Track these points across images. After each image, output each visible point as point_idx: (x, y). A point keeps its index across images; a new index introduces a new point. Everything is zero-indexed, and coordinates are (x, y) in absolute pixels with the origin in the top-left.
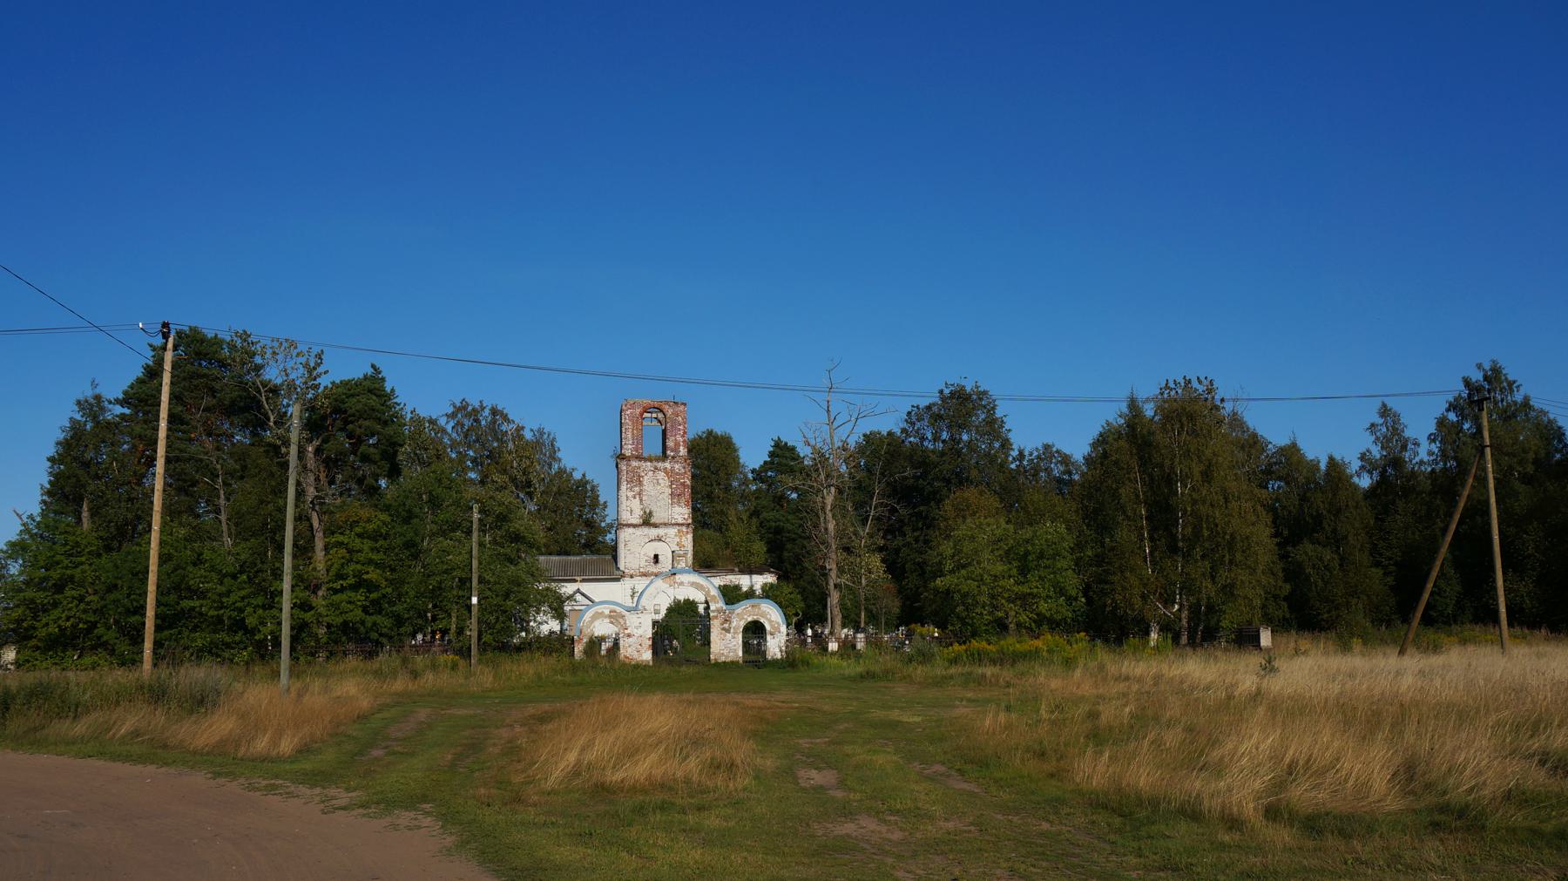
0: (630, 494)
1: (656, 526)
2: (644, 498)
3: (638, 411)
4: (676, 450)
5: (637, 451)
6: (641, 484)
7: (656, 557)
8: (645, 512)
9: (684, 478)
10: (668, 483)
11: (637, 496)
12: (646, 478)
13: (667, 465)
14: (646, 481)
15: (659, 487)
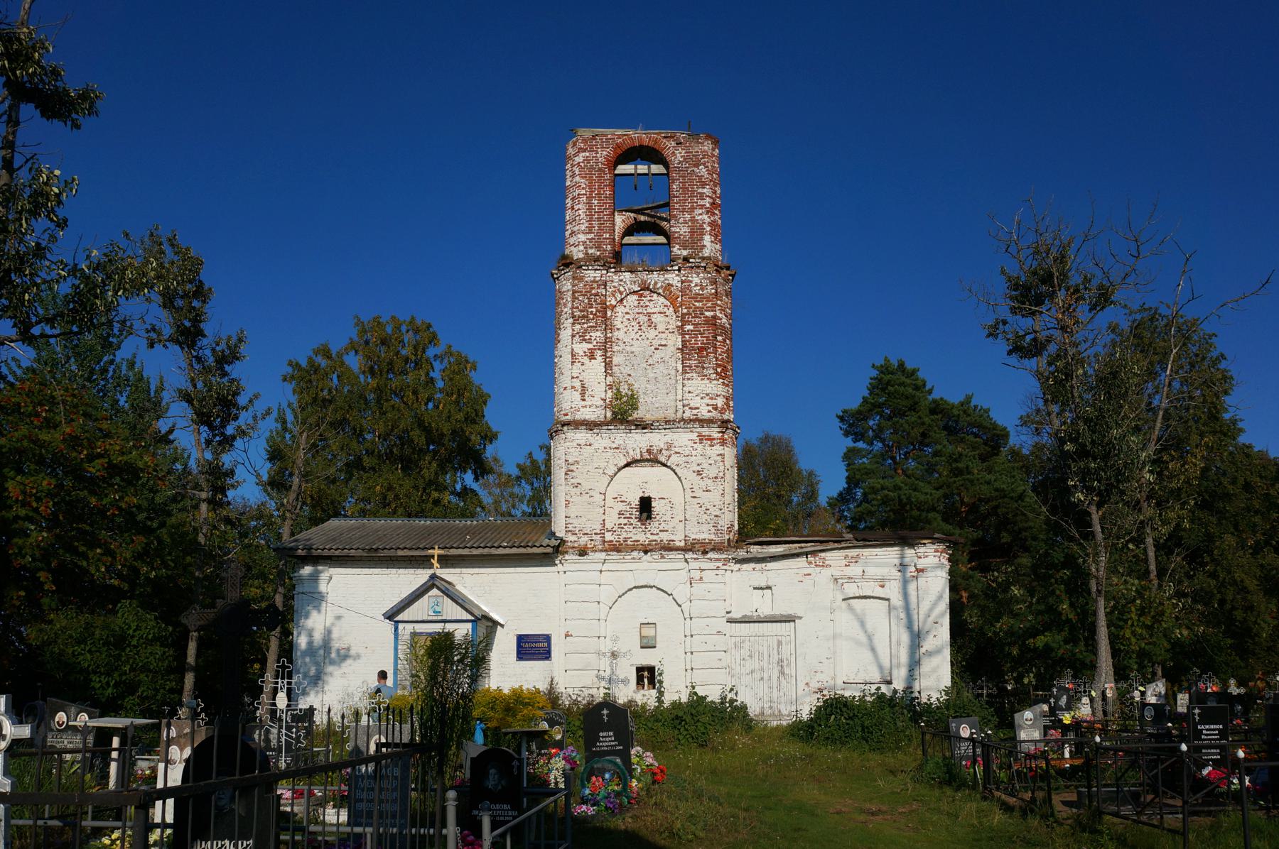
0: (581, 348)
1: (643, 426)
2: (616, 360)
3: (603, 155)
4: (694, 241)
5: (598, 248)
6: (607, 325)
7: (645, 506)
8: (618, 395)
9: (713, 309)
10: (674, 323)
12: (620, 309)
13: (674, 279)
14: (619, 318)
15: (652, 333)
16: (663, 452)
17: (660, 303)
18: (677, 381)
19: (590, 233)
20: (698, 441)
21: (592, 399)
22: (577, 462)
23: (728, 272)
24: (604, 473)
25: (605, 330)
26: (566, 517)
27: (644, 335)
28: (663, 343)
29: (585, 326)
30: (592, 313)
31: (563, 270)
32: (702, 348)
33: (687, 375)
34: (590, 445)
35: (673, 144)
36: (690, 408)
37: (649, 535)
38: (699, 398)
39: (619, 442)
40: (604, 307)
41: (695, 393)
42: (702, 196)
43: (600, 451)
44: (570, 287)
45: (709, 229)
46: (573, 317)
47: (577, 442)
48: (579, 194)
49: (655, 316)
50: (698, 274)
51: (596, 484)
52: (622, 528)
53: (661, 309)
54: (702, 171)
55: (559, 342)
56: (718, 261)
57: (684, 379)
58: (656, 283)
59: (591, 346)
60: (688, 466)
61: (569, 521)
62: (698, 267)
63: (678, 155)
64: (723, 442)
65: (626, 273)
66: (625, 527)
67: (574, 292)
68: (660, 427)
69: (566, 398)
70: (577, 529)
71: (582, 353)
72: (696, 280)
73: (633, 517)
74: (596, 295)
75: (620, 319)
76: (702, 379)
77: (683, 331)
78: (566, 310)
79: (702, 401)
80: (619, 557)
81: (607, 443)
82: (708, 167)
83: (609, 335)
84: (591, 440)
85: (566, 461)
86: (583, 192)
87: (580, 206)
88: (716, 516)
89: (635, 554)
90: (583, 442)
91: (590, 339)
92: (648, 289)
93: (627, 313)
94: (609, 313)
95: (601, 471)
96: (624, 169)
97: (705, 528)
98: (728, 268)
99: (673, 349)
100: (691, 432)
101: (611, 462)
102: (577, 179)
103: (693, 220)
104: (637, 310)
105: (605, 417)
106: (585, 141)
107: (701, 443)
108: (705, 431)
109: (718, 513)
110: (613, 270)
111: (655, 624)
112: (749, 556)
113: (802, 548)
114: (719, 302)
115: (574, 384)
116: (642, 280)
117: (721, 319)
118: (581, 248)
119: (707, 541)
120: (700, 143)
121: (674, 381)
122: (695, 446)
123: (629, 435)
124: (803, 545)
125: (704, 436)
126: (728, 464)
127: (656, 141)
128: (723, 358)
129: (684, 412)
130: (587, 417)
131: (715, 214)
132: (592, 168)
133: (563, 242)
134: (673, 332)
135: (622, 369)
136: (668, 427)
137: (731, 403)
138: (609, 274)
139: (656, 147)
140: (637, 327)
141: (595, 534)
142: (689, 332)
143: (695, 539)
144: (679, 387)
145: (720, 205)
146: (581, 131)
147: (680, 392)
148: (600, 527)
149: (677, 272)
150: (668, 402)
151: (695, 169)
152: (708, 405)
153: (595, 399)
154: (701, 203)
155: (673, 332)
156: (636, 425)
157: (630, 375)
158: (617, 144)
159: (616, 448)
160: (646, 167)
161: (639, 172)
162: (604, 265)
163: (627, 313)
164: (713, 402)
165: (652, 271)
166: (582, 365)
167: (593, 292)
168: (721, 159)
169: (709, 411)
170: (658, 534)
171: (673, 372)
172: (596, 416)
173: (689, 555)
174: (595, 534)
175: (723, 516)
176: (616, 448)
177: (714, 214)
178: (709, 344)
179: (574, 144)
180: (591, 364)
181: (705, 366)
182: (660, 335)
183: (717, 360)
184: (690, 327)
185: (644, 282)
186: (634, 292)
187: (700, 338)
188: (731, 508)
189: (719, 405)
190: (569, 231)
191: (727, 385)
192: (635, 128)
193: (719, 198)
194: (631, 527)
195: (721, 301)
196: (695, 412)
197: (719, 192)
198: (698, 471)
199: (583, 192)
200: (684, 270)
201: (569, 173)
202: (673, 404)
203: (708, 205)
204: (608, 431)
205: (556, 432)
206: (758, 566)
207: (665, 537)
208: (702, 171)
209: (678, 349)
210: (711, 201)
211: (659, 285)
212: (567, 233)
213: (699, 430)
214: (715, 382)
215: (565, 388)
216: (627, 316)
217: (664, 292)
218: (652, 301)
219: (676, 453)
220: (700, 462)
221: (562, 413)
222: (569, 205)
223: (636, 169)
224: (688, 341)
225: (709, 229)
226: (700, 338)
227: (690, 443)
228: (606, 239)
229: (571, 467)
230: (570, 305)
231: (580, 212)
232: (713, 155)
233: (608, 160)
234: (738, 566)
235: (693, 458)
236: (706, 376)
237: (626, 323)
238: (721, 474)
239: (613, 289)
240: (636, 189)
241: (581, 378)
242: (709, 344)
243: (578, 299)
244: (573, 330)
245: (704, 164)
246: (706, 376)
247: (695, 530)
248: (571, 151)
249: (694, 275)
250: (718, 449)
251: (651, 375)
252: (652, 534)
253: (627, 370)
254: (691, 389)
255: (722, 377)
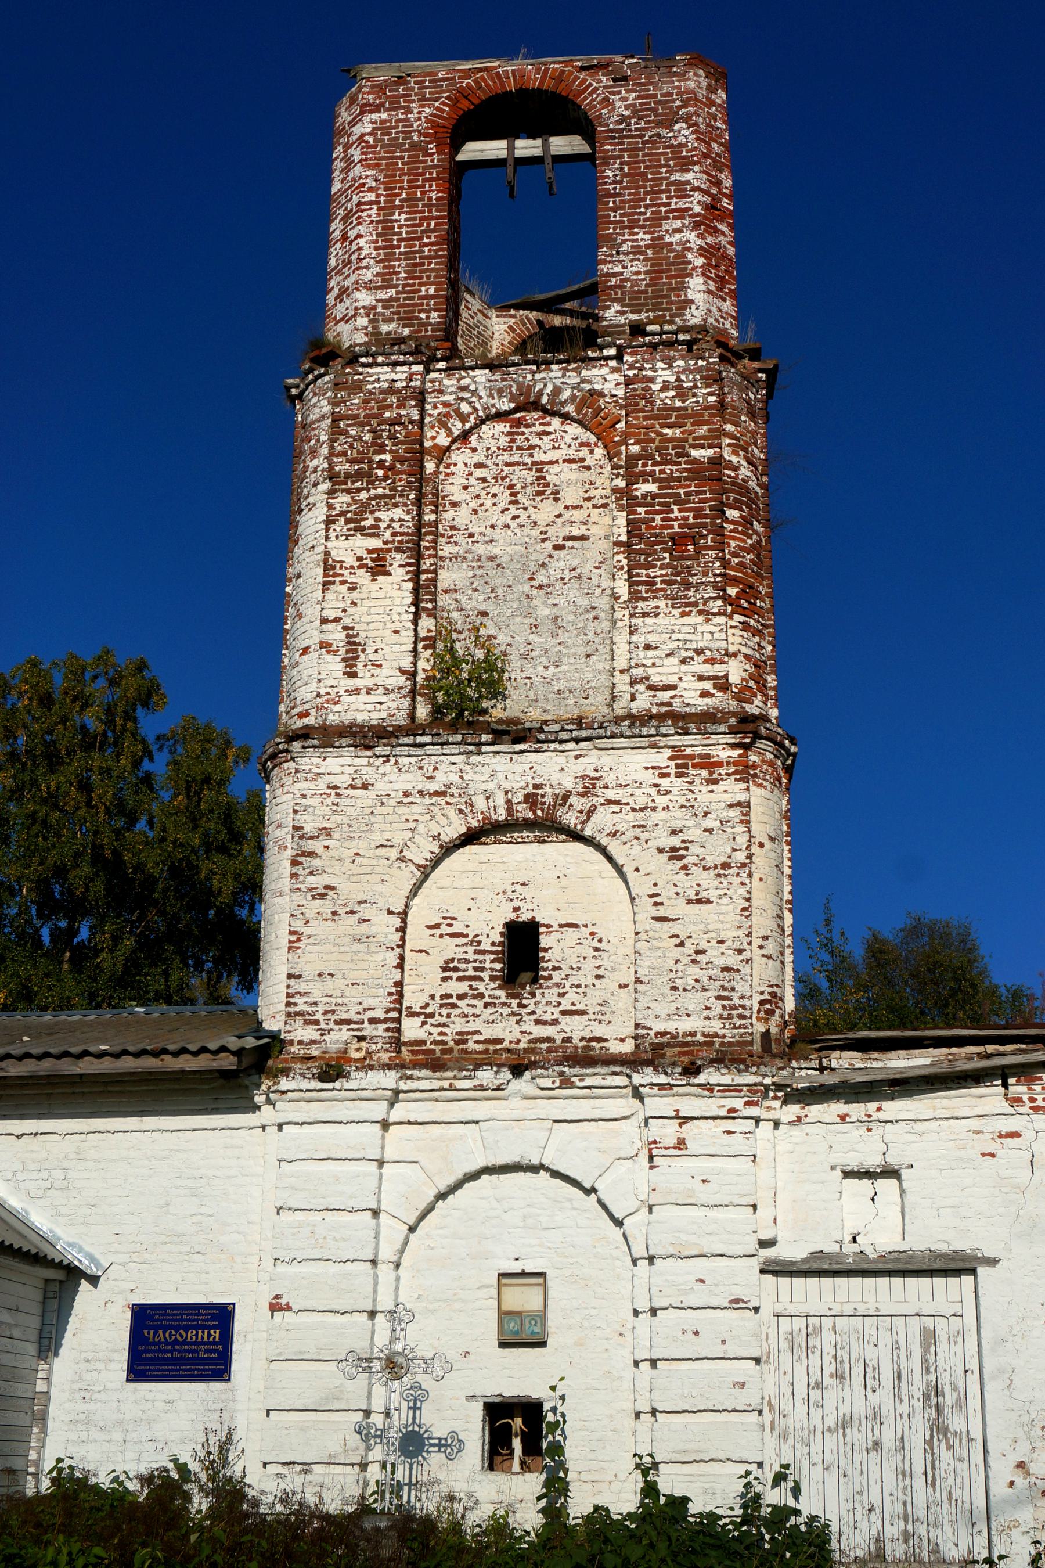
2: (445, 578)
5: (407, 319)
9: (713, 440)
11: (397, 560)
12: (460, 457)
15: (547, 510)
16: (573, 800)
17: (568, 439)
18: (614, 622)
19: (387, 285)
20: (672, 771)
21: (376, 671)
22: (327, 832)
23: (756, 365)
24: (402, 859)
25: (419, 502)
26: (290, 976)
27: (524, 515)
28: (576, 532)
29: (364, 495)
30: (381, 464)
31: (311, 370)
32: (683, 536)
33: (641, 604)
34: (365, 787)
35: (605, 81)
36: (650, 688)
37: (529, 1026)
38: (674, 661)
39: (442, 779)
40: (417, 453)
41: (666, 649)
42: (682, 190)
43: (392, 802)
44: (327, 409)
45: (700, 261)
46: (333, 476)
47: (331, 778)
48: (359, 204)
49: (555, 469)
50: (669, 362)
51: (380, 888)
52: (454, 1006)
53: (572, 453)
54: (683, 133)
55: (296, 542)
56: (728, 335)
57: (632, 616)
58: (557, 391)
59: (376, 543)
60: (644, 836)
61: (298, 986)
62: (671, 344)
63: (618, 104)
64: (745, 772)
65: (478, 372)
66: (460, 1003)
67: (336, 418)
68: (564, 735)
69: (305, 673)
70: (321, 1009)
71: (350, 561)
72: (665, 375)
73: (485, 975)
74: (393, 423)
75: (459, 480)
76: (683, 615)
77: (631, 497)
78: (315, 462)
79: (684, 668)
80: (436, 1084)
81: (412, 780)
82: (696, 124)
83: (429, 517)
84: (369, 774)
85: (296, 828)
86: (371, 197)
87: (362, 229)
88: (727, 969)
89: (486, 1076)
90: (343, 780)
91: (377, 527)
92: (535, 405)
93: (479, 465)
94: (430, 466)
95: (394, 854)
96: (475, 150)
97: (693, 1001)
98: (755, 355)
99: (604, 545)
100: (653, 746)
101: (421, 828)
102: (358, 170)
103: (658, 245)
104: (506, 457)
105: (412, 715)
106: (379, 89)
107: (679, 775)
108: (694, 744)
109: (733, 960)
110: (442, 365)
111: (542, 1275)
112: (829, 1079)
113: (989, 1056)
114: (729, 427)
115: (328, 637)
116: (519, 384)
117: (736, 469)
118: (363, 321)
119: (699, 1038)
120: (676, 74)
121: (606, 625)
122: (665, 782)
123: (474, 759)
124: (991, 1049)
125: (692, 757)
126: (760, 831)
127: (560, 78)
128: (741, 564)
129: (633, 698)
130: (360, 718)
131: (716, 231)
132: (395, 144)
133: (319, 312)
134: (605, 506)
135: (464, 600)
136: (584, 734)
137: (771, 680)
138: (433, 375)
139: (561, 89)
140: (505, 497)
141: (373, 1021)
142: (647, 499)
143: (658, 1034)
144: (621, 638)
145: (731, 214)
146: (368, 70)
147: (622, 649)
148: (386, 1002)
149: (613, 363)
150: (589, 676)
151: (664, 132)
152: (701, 678)
153: (385, 671)
154: (682, 204)
155: (605, 506)
156: (494, 732)
157: (484, 614)
158: (460, 90)
159: (437, 794)
160: (538, 142)
161: (519, 153)
162: (417, 352)
163: (479, 465)
164: (718, 670)
165: (548, 363)
166: (353, 588)
167: (387, 415)
168: (733, 113)
169: (705, 694)
170: (555, 1022)
171: (604, 603)
172: (384, 715)
173: (646, 1077)
174: (373, 1021)
175: (746, 969)
176: (437, 794)
177: (716, 231)
178: (704, 526)
179: (353, 100)
180: (375, 586)
181: (693, 580)
182: (567, 515)
183: (725, 564)
184: (652, 487)
185: (525, 390)
186: (500, 416)
187: (676, 513)
188: (771, 947)
189: (734, 678)
190: (336, 291)
191: (756, 633)
192: (508, 54)
193: (725, 195)
194: (480, 1003)
195: (736, 424)
196: (664, 696)
197: (728, 183)
198: (674, 849)
199: (371, 197)
200: (632, 354)
201: (338, 165)
202: (604, 680)
203: (697, 209)
204: (414, 751)
205: (273, 756)
206: (856, 1110)
207: (576, 1029)
208: (683, 133)
209: (617, 544)
210: (707, 199)
211: (566, 394)
212: (331, 298)
213: (677, 740)
214: (722, 619)
215: (305, 651)
216: (479, 473)
217: (578, 410)
218: (548, 433)
219: (610, 802)
220: (677, 825)
221: (295, 711)
222: (337, 232)
223: (511, 148)
224: (644, 521)
225: (700, 261)
226: (676, 513)
227: (650, 777)
228: (428, 297)
229: (310, 846)
230: (325, 450)
231: (362, 242)
232: (713, 103)
233: (435, 125)
234: (794, 1110)
235: (659, 816)
236: (695, 604)
237: (477, 488)
238: (740, 857)
239: (441, 409)
240: (511, 195)
241: (347, 621)
242: (704, 526)
243: (346, 433)
244: (330, 507)
245: (687, 120)
246: (695, 604)
247: (663, 1008)
248: (344, 116)
249: (660, 365)
250: (731, 789)
251: (544, 612)
252: (538, 1022)
253: (478, 602)
254: (652, 639)
255: (739, 610)
